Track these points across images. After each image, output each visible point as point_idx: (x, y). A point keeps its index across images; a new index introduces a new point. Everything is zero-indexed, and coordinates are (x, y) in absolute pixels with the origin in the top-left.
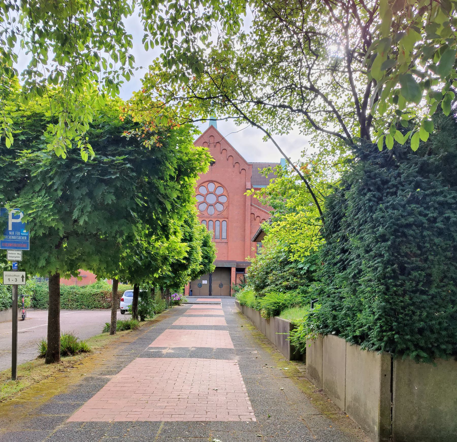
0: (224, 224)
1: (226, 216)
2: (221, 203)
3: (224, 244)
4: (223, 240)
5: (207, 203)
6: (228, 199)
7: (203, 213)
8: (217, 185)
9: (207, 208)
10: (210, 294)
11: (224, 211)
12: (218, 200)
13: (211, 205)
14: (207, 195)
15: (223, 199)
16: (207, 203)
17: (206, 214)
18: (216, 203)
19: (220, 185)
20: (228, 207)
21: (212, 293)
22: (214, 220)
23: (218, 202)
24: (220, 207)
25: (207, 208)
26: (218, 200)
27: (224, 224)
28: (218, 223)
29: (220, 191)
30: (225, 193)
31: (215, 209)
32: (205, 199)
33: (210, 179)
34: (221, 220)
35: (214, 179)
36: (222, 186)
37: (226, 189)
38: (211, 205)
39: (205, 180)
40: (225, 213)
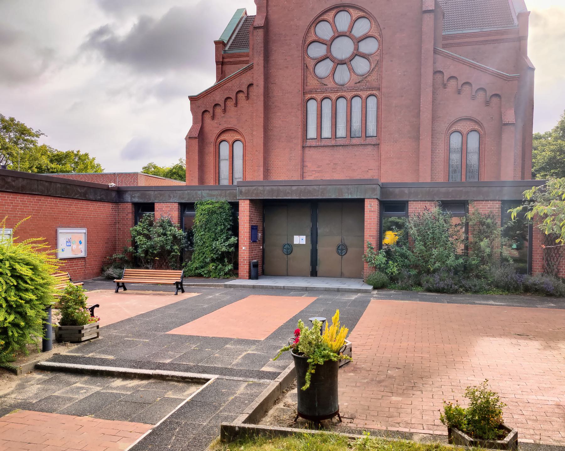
0: (372, 103)
2: (364, 56)
3: (370, 148)
4: (369, 141)
5: (333, 60)
6: (380, 43)
8: (356, 13)
11: (370, 73)
13: (342, 63)
14: (334, 39)
16: (333, 60)
17: (331, 85)
18: (352, 58)
23: (357, 54)
26: (357, 48)
27: (372, 103)
29: (362, 27)
31: (351, 70)
32: (329, 50)
34: (364, 94)
36: (366, 15)
37: (376, 21)
38: (342, 63)
39: (328, 6)
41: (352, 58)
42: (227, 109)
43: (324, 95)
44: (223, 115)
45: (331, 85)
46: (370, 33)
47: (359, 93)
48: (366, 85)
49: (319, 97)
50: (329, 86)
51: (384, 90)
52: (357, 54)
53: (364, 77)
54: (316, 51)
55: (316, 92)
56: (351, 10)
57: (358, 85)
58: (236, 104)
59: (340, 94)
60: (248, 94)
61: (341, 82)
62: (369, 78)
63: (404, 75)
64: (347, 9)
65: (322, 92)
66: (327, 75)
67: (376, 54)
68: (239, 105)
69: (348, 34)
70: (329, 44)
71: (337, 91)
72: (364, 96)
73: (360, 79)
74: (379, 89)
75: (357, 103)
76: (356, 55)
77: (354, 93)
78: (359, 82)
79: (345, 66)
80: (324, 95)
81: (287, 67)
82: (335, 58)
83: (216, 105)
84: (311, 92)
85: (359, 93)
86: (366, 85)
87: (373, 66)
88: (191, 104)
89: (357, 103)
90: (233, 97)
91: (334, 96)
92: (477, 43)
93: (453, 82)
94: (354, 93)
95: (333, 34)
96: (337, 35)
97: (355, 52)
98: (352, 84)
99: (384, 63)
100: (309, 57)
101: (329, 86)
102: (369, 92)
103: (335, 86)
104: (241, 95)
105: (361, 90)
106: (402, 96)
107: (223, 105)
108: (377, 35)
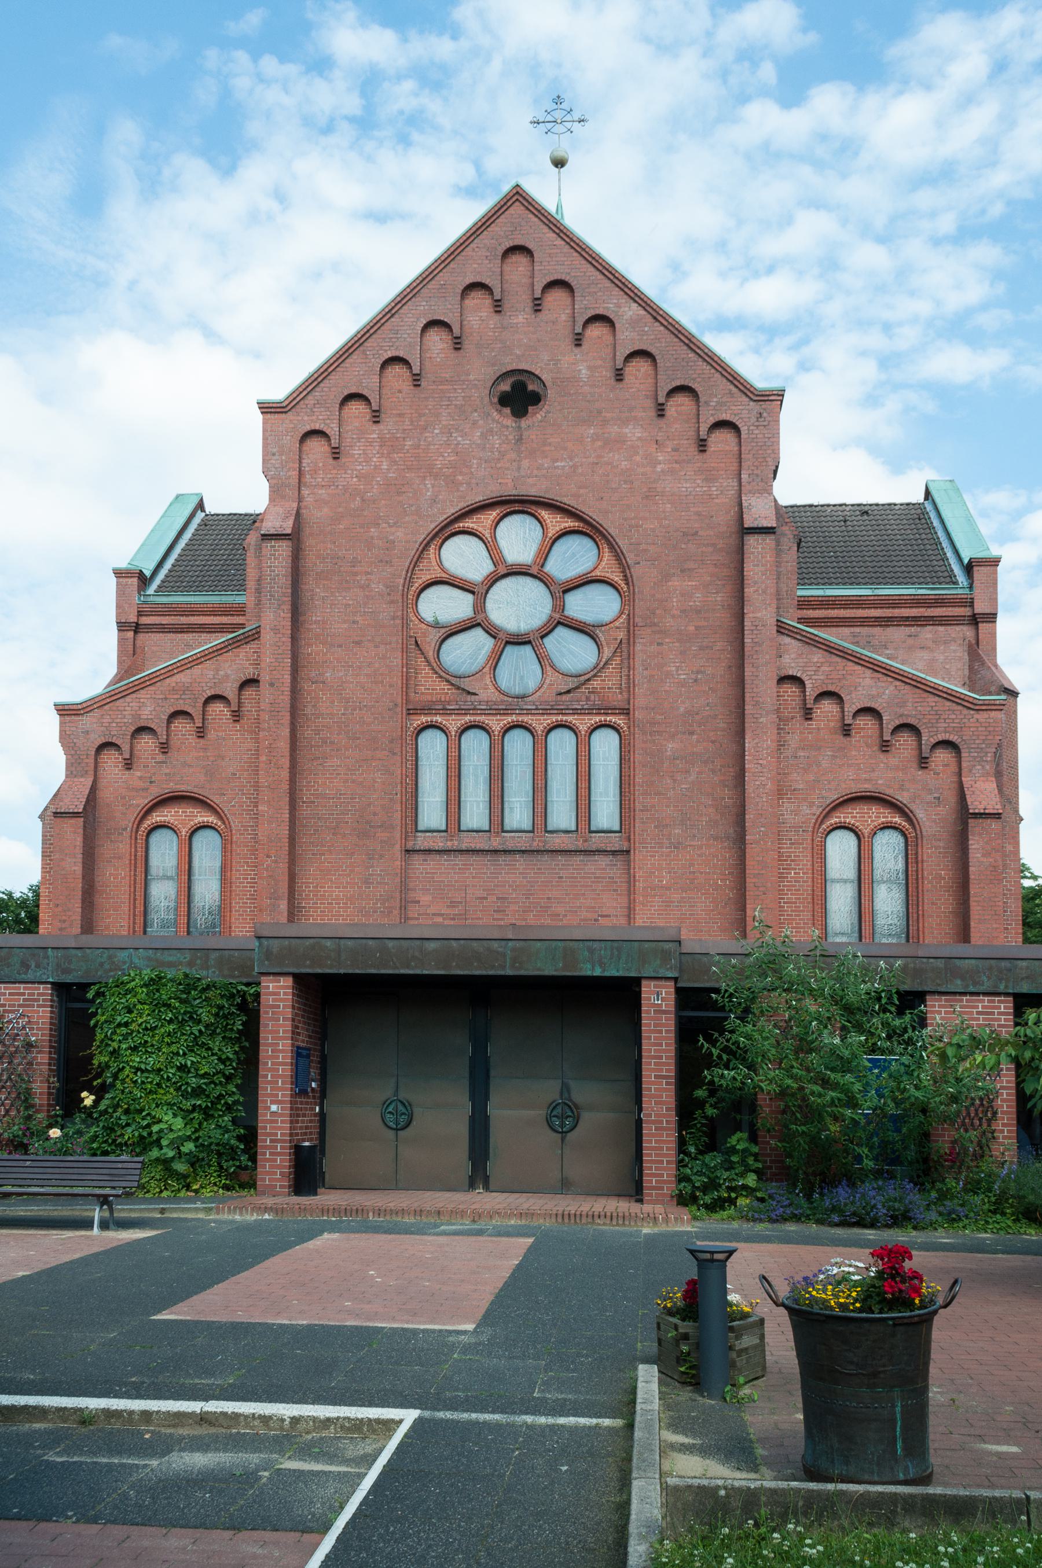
1: (617, 699)
7: (465, 684)
8: (556, 523)
9: (495, 658)
11: (598, 669)
12: (559, 606)
13: (518, 640)
15: (596, 605)
16: (492, 631)
17: (486, 693)
18: (546, 631)
19: (570, 523)
20: (625, 649)
22: (540, 723)
23: (560, 621)
24: (574, 653)
25: (495, 658)
27: (605, 747)
28: (562, 745)
29: (574, 557)
30: (608, 569)
33: (509, 488)
34: (583, 723)
35: (533, 488)
40: (609, 683)
41: (546, 631)
42: (174, 741)
43: (468, 718)
44: (161, 757)
45: (486, 693)
46: (598, 573)
47: (570, 718)
48: (588, 699)
49: (454, 724)
50: (483, 695)
51: (638, 715)
52: (560, 621)
53: (583, 679)
54: (443, 606)
55: (445, 712)
56: (544, 514)
57: (565, 697)
58: (201, 733)
59: (514, 717)
60: (240, 704)
61: (517, 690)
62: (595, 683)
63: (696, 680)
64: (532, 509)
65: (462, 712)
66: (475, 668)
67: (617, 624)
68: (212, 735)
69: (534, 571)
70: (479, 591)
71: (506, 712)
72: (583, 728)
73: (571, 684)
74: (626, 712)
75: (562, 747)
76: (559, 623)
77: (554, 719)
78: (568, 692)
79: (528, 649)
80: (468, 718)
81: (358, 643)
82: (499, 629)
83: (141, 730)
84: (426, 709)
85: (570, 718)
86: (588, 699)
87: (607, 653)
88: (62, 724)
89: (562, 745)
90: (196, 711)
91: (496, 724)
92: (864, 622)
93: (828, 706)
94: (554, 719)
95: (492, 568)
96: (502, 571)
97: (557, 616)
98: (548, 695)
99: (638, 647)
100: (421, 620)
101: (483, 695)
102: (597, 719)
103: (496, 696)
104: (218, 707)
105: (575, 712)
106: (692, 733)
107: (161, 731)
108: (617, 578)
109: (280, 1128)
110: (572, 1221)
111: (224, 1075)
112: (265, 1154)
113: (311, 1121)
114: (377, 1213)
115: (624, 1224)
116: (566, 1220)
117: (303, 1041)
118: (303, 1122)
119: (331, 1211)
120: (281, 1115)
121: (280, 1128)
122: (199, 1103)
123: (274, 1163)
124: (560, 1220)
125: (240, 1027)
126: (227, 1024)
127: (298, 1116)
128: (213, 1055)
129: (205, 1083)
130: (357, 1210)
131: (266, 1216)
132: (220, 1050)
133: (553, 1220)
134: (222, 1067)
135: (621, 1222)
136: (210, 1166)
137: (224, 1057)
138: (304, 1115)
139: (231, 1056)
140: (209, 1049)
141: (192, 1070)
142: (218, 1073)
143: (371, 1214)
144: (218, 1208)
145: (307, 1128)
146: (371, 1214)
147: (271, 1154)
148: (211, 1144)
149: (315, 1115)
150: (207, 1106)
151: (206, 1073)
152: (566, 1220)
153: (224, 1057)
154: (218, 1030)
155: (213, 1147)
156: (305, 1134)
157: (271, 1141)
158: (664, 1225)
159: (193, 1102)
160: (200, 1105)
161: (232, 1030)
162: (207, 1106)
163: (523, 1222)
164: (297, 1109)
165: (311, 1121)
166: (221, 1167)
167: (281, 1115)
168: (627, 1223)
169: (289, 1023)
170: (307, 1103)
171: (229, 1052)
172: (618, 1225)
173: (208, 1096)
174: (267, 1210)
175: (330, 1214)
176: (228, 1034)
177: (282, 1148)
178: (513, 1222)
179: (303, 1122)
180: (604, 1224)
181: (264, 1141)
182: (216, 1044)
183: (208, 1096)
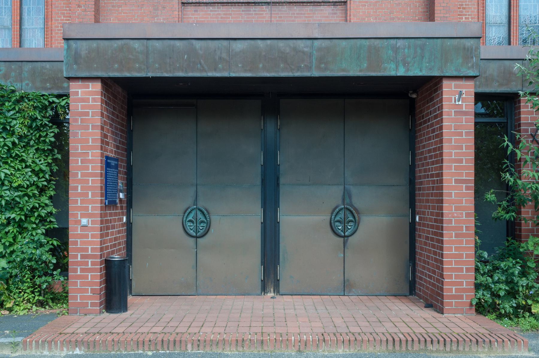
10: (270, 277)
21: (286, 272)
109: (90, 243)
110: (404, 348)
111: (38, 187)
112: (75, 271)
113: (119, 232)
114: (196, 343)
115: (458, 350)
116: (397, 347)
117: (111, 151)
118: (112, 234)
119: (146, 344)
120: (92, 229)
121: (90, 243)
122: (13, 216)
123: (85, 279)
124: (390, 347)
125: (53, 139)
126: (40, 136)
127: (108, 228)
128: (26, 167)
129: (19, 196)
130: (175, 341)
131: (77, 351)
132: (33, 162)
133: (384, 347)
134: (35, 179)
135: (454, 348)
136: (23, 282)
137: (37, 169)
138: (113, 227)
139: (44, 168)
140: (23, 161)
141: (6, 183)
142: (32, 185)
143: (189, 346)
144: (25, 342)
145: (116, 239)
146: (189, 346)
147: (82, 270)
148: (23, 260)
149: (123, 225)
150: (21, 219)
151: (20, 186)
152: (397, 347)
153: (37, 169)
154: (32, 143)
155: (26, 263)
156: (115, 245)
157: (83, 257)
158: (500, 350)
159: (8, 215)
160: (14, 219)
161: (44, 142)
162: (21, 219)
163: (352, 351)
164: (107, 221)
165: (119, 232)
166: (34, 284)
167: (92, 229)
168: (461, 348)
169: (99, 131)
170: (116, 214)
171: (42, 164)
172: (451, 351)
173: (21, 209)
174: (77, 343)
175: (146, 347)
176: (41, 146)
177: (93, 264)
178: (340, 351)
179: (112, 234)
180: (437, 351)
181: (75, 257)
182: (30, 156)
183: (21, 209)
